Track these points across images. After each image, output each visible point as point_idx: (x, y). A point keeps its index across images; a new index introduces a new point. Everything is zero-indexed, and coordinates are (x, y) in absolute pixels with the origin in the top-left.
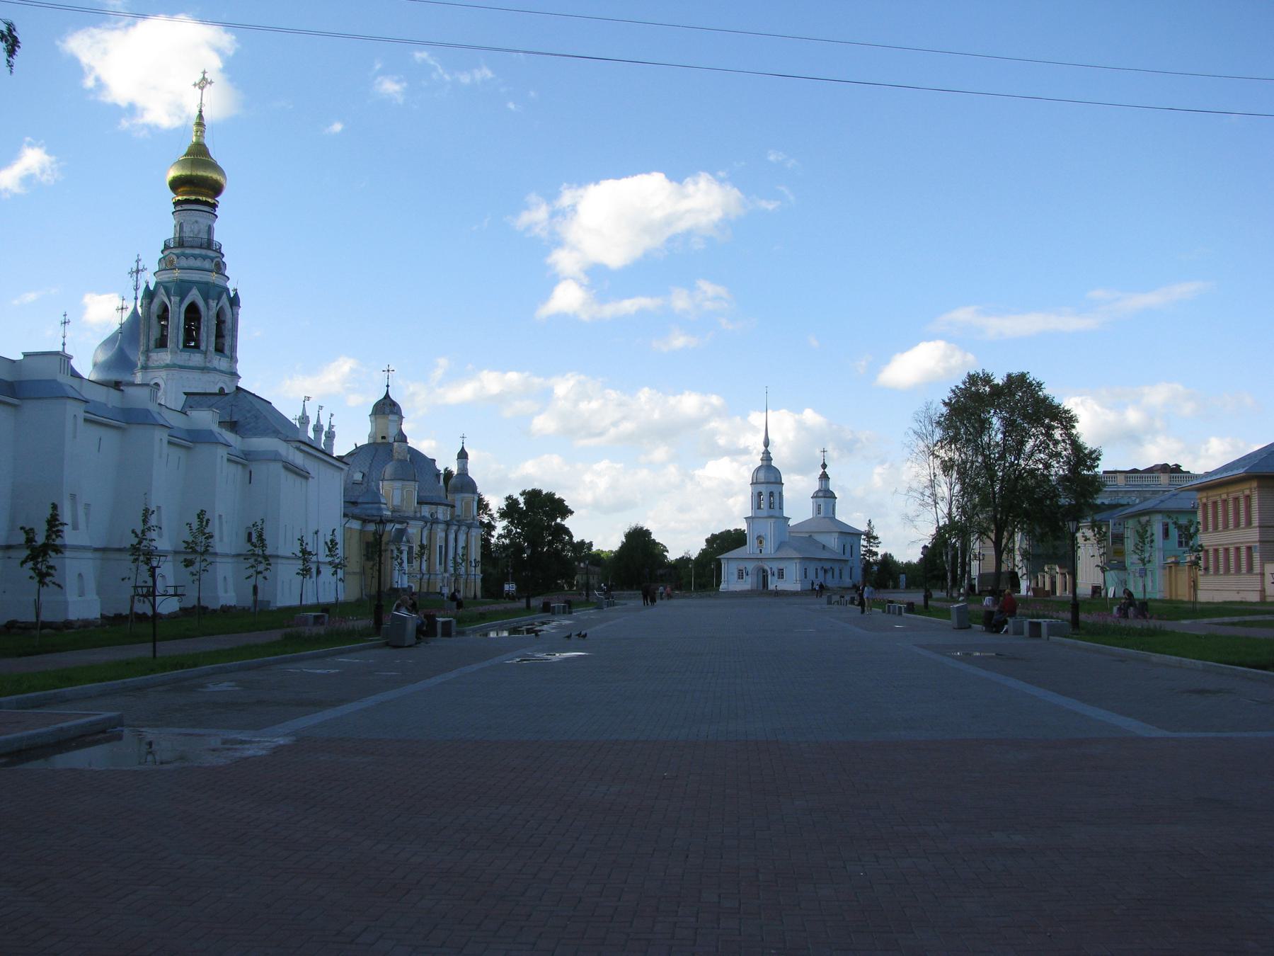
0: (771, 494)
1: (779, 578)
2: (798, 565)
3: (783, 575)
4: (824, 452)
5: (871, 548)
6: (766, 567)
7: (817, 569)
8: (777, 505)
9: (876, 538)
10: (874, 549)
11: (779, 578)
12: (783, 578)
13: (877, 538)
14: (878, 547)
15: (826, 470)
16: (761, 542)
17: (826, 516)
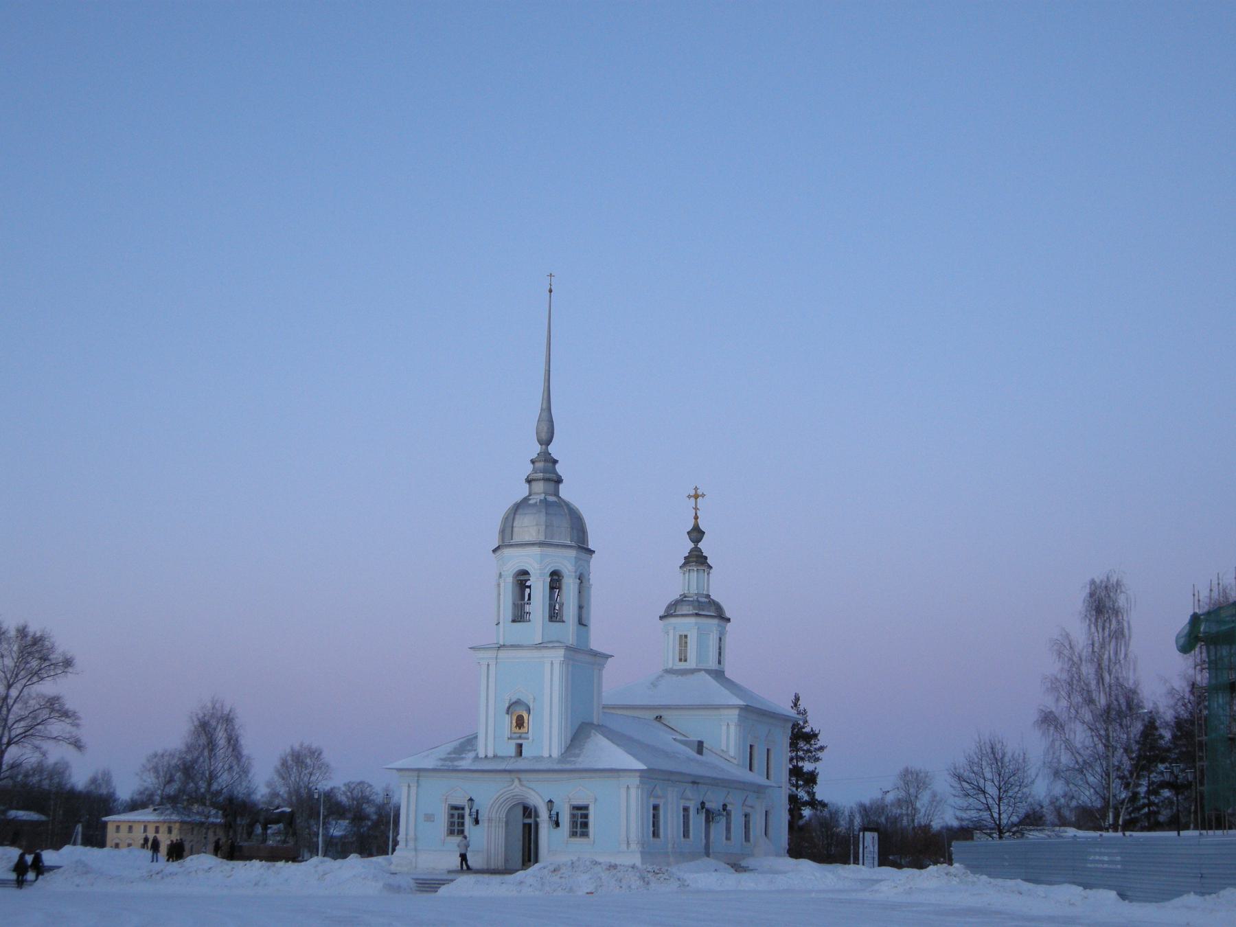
0: (555, 579)
1: (574, 834)
2: (633, 791)
3: (585, 825)
4: (696, 497)
5: (800, 764)
6: (537, 800)
7: (686, 809)
8: (570, 612)
9: (811, 737)
10: (807, 766)
11: (574, 834)
12: (585, 834)
13: (815, 736)
14: (817, 759)
15: (700, 545)
16: (520, 722)
17: (701, 666)
